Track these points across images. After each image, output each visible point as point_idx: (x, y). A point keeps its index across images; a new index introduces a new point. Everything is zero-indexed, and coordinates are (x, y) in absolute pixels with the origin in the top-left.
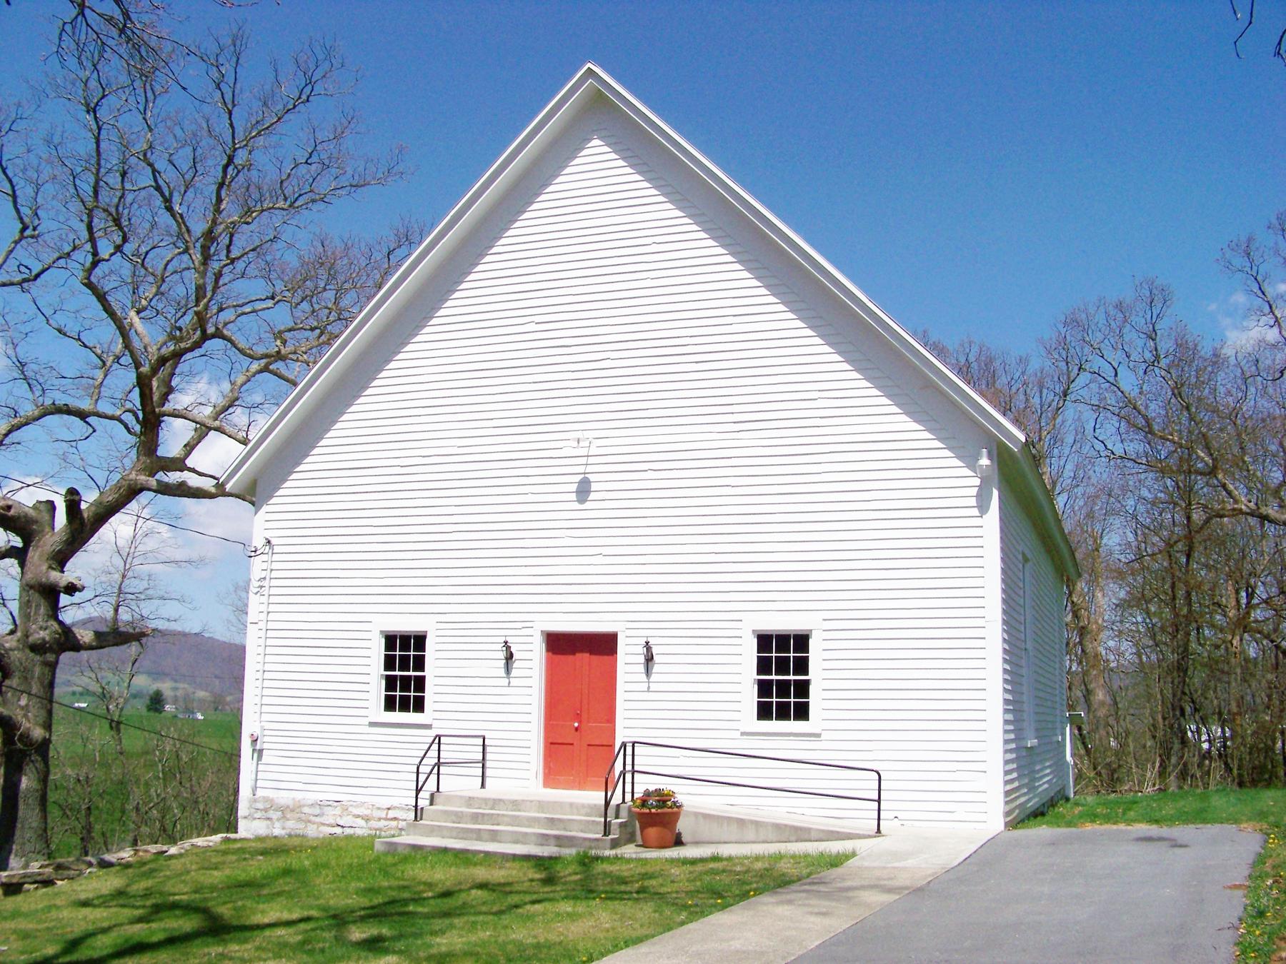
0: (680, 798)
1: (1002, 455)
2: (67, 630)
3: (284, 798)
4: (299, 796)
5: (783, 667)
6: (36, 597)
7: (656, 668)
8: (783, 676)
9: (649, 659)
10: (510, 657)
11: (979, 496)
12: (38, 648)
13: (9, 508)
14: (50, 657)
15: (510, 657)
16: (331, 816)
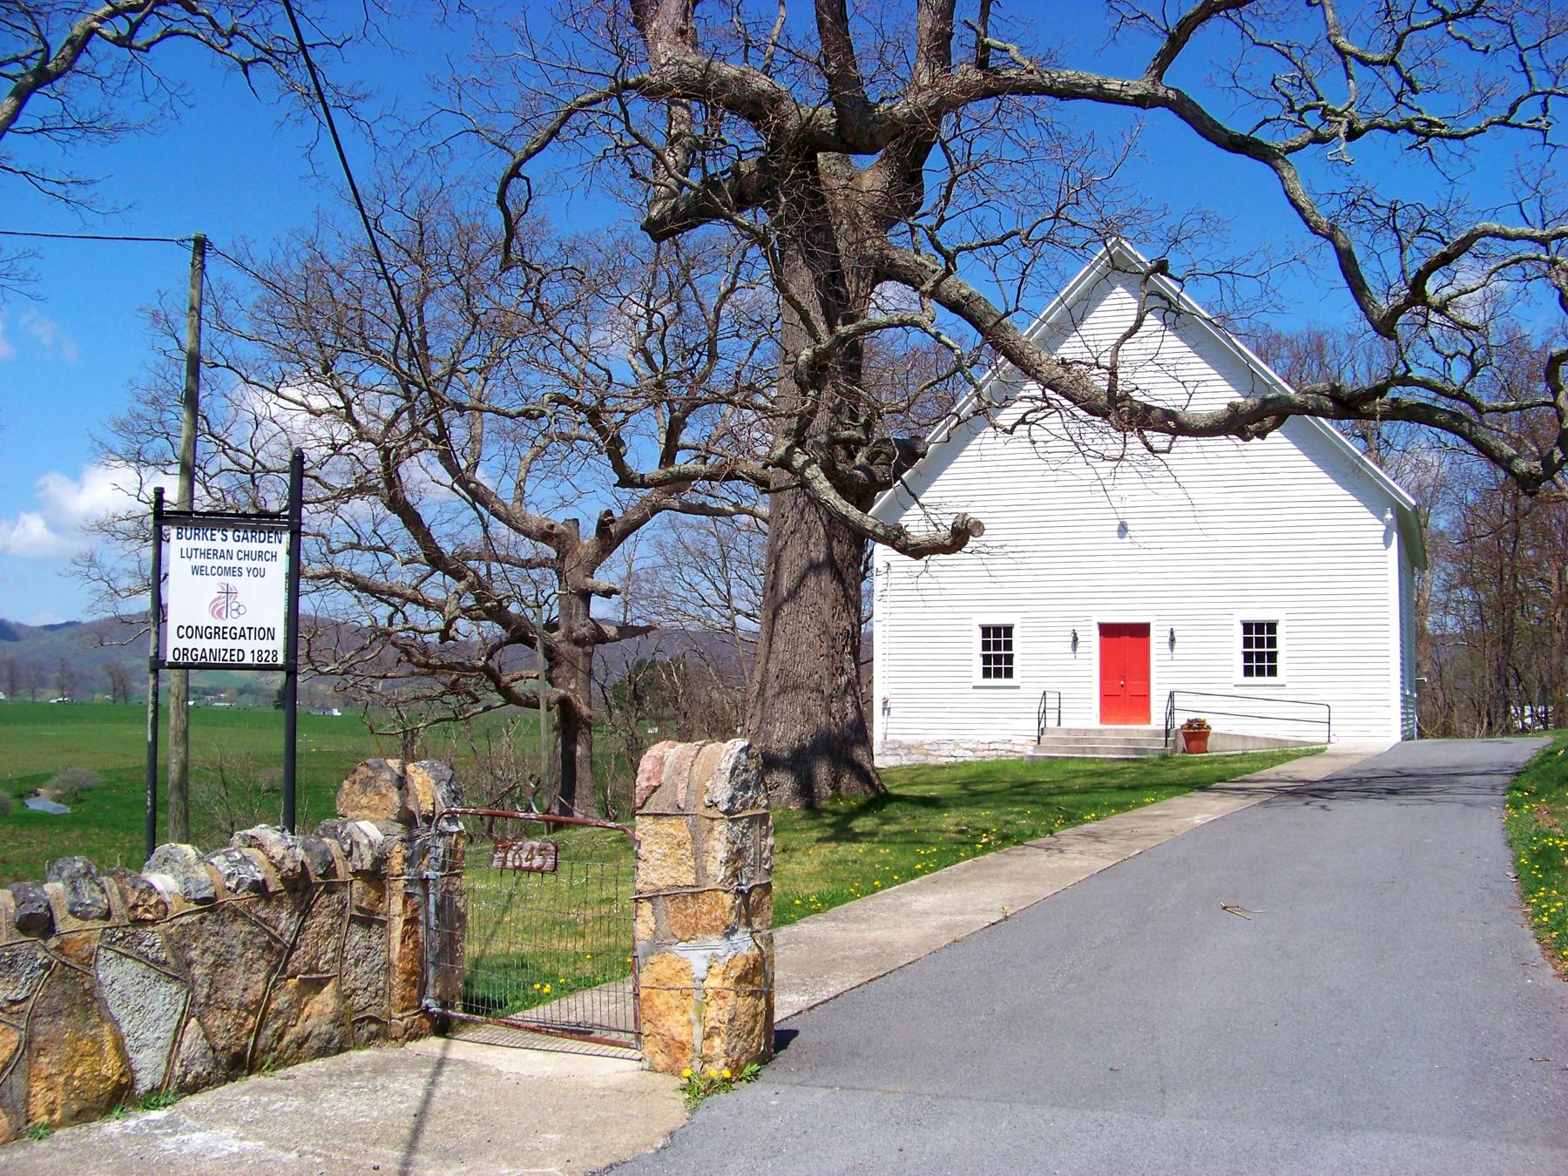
0: (1208, 722)
1: (1399, 511)
2: (597, 625)
3: (906, 740)
4: (920, 738)
5: (997, 646)
6: (575, 600)
7: (1176, 645)
8: (1260, 648)
9: (1172, 640)
10: (1075, 640)
11: (1385, 537)
12: (579, 642)
13: (552, 527)
14: (588, 649)
15: (1075, 640)
16: (945, 750)
